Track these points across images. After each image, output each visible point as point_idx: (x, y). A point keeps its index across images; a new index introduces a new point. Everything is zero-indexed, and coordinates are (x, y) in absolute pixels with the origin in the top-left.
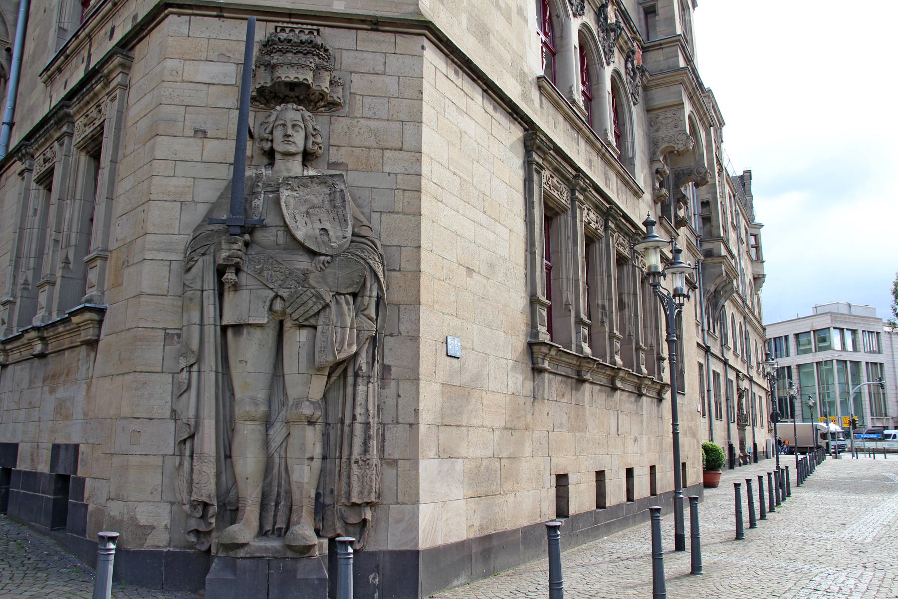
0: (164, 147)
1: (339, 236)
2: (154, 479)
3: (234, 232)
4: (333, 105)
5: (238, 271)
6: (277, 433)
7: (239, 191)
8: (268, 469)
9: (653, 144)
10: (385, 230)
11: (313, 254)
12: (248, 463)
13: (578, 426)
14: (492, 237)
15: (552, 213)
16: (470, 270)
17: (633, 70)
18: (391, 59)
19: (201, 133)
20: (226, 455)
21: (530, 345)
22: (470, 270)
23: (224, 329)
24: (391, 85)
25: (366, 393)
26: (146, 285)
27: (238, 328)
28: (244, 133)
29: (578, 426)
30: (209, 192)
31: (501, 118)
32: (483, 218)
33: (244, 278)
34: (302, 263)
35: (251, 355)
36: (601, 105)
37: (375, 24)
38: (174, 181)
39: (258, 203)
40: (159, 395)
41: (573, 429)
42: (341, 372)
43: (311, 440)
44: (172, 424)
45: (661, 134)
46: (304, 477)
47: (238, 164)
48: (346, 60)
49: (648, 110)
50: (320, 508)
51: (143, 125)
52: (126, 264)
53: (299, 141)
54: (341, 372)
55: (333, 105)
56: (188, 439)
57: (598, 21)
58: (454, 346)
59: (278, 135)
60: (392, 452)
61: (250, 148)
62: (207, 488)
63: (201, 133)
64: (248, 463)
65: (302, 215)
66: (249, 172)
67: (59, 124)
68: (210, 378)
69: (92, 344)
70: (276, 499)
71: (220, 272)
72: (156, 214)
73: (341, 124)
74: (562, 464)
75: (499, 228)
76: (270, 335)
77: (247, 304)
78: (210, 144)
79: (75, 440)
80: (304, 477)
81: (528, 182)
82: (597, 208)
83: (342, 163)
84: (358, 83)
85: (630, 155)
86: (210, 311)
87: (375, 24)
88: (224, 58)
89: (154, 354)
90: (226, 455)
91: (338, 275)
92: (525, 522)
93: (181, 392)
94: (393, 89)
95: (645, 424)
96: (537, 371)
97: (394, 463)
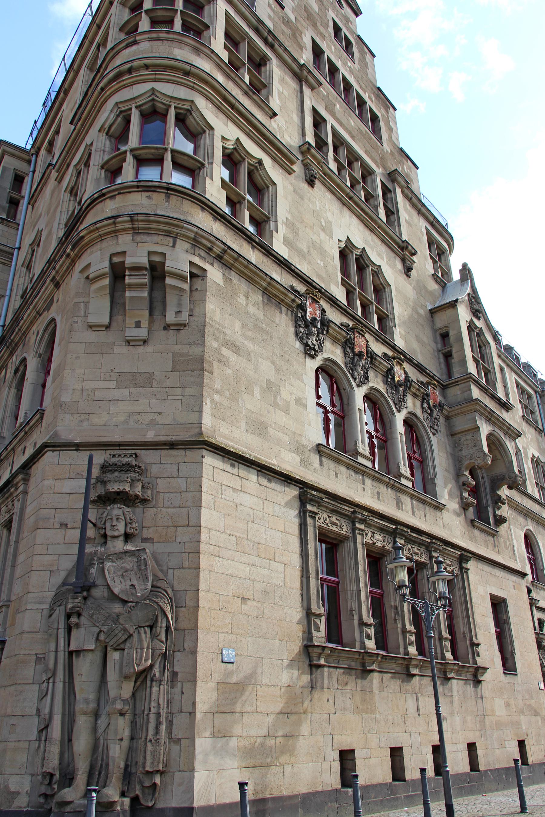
0: (42, 536)
1: (142, 588)
2: (22, 758)
4: (144, 501)
5: (79, 615)
6: (102, 722)
7: (82, 564)
8: (95, 748)
9: (457, 463)
10: (177, 579)
11: (124, 602)
12: (82, 744)
13: (366, 707)
14: (266, 572)
15: (332, 544)
16: (244, 600)
17: (429, 408)
18: (183, 467)
19: (64, 526)
20: (68, 738)
21: (306, 647)
22: (244, 600)
23: (71, 653)
24: (181, 483)
25: (159, 693)
26: (26, 628)
27: (78, 652)
29: (366, 707)
30: (68, 563)
31: (276, 486)
32: (256, 560)
33: (84, 620)
34: (118, 608)
35: (86, 669)
36: (394, 445)
37: (172, 445)
38: (47, 558)
39: (93, 571)
41: (358, 711)
42: (143, 677)
43: (122, 726)
44: (36, 720)
45: (464, 453)
46: (117, 753)
48: (154, 470)
49: (452, 434)
50: (127, 775)
51: (32, 519)
52: (18, 611)
53: (121, 528)
54: (143, 677)
55: (144, 501)
57: (386, 382)
58: (229, 654)
59: (108, 525)
60: (177, 733)
61: (91, 533)
62: (53, 763)
63: (64, 526)
64: (82, 744)
65: (117, 578)
66: (89, 549)
68: (60, 686)
71: (68, 616)
72: (35, 579)
73: (150, 512)
75: (273, 565)
76: (97, 657)
78: (70, 532)
80: (117, 753)
82: (382, 530)
83: (150, 538)
84: (161, 485)
85: (432, 475)
86: (62, 642)
87: (172, 445)
88: (79, 476)
89: (29, 672)
91: (139, 615)
92: (304, 789)
93: (42, 697)
94: (183, 487)
95: (456, 704)
96: (314, 667)
97: (178, 741)
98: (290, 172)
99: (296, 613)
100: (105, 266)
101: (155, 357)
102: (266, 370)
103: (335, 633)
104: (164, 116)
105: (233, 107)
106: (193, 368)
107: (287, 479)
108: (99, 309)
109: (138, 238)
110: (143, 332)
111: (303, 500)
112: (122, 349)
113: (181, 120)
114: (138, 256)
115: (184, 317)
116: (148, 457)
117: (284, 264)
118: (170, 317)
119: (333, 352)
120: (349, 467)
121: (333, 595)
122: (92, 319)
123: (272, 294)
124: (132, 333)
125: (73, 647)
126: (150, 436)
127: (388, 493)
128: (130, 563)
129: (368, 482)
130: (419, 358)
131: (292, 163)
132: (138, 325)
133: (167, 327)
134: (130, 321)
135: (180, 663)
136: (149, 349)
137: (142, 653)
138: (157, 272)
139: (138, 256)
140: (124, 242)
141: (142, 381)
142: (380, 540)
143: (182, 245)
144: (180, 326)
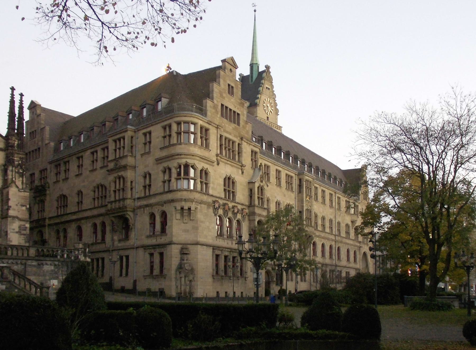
1: (190, 268)
3: (180, 268)
20: (181, 288)
25: (193, 283)
28: (181, 258)
31: (209, 248)
35: (183, 279)
40: (173, 283)
42: (190, 281)
43: (188, 287)
47: (181, 260)
50: (189, 293)
56: (177, 287)
57: (232, 214)
63: (176, 258)
64: (183, 289)
65: (187, 266)
67: (154, 248)
69: (165, 278)
70: (185, 293)
74: (218, 290)
77: (183, 275)
82: (228, 251)
84: (191, 251)
87: (193, 244)
89: (173, 279)
90: (181, 288)
93: (176, 283)
96: (214, 278)
98: (213, 166)
100: (180, 208)
101: (189, 226)
102: (207, 224)
103: (217, 273)
106: (196, 229)
108: (178, 216)
111: (213, 249)
112: (183, 224)
113: (192, 167)
114: (186, 208)
115: (194, 218)
116: (189, 246)
117: (212, 196)
118: (191, 218)
119: (221, 212)
121: (217, 265)
122: (177, 218)
123: (208, 205)
124: (185, 221)
126: (189, 242)
127: (230, 242)
128: (188, 264)
129: (226, 240)
130: (243, 202)
133: (191, 220)
134: (184, 219)
135: (195, 278)
136: (187, 225)
137: (191, 277)
138: (189, 209)
139: (186, 208)
140: (183, 204)
141: (186, 231)
142: (227, 254)
143: (194, 203)
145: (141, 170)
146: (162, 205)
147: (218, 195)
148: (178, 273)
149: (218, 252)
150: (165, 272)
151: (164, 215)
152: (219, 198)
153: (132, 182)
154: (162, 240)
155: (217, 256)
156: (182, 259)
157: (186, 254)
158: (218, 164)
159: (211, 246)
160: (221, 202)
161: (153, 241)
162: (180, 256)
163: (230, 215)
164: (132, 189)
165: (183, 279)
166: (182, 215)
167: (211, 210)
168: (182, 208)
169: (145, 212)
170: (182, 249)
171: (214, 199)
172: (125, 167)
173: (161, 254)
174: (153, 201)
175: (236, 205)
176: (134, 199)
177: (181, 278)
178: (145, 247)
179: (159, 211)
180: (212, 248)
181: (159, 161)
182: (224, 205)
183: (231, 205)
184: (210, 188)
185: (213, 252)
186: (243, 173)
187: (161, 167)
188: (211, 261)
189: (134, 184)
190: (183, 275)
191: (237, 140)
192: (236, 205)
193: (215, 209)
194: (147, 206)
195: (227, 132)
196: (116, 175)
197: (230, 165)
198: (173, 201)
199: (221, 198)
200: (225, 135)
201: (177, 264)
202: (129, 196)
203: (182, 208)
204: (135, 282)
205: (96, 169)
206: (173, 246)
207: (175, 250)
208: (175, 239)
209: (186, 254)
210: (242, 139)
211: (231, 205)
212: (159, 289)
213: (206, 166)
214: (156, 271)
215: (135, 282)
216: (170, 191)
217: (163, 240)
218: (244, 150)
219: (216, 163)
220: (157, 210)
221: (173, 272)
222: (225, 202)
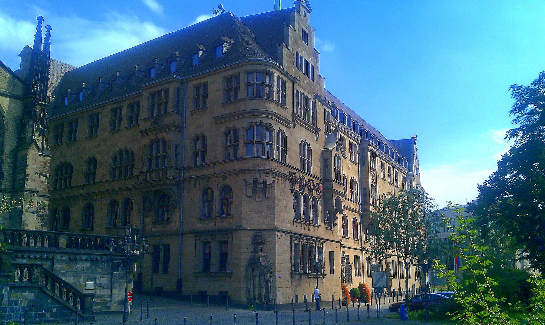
3: (253, 263)
4: (264, 243)
31: (287, 235)
34: (263, 268)
35: (257, 279)
37: (269, 230)
40: (244, 285)
56: (249, 290)
64: (257, 293)
69: (230, 277)
70: (260, 297)
72: (242, 260)
77: (257, 273)
79: (226, 290)
81: (291, 243)
93: (247, 284)
96: (292, 277)
99: (290, 266)
104: (263, 126)
105: (280, 119)
106: (272, 209)
107: (288, 233)
108: (250, 192)
109: (261, 175)
110: (260, 199)
111: (291, 237)
112: (255, 203)
115: (270, 195)
116: (264, 232)
117: (289, 166)
118: (267, 195)
119: (297, 187)
120: (299, 223)
122: (248, 194)
124: (258, 199)
125: (254, 275)
131: (289, 124)
132: (259, 197)
133: (266, 197)
134: (257, 196)
135: (273, 278)
138: (265, 182)
140: (257, 175)
144: (269, 197)
145: (191, 131)
146: (226, 178)
147: (294, 166)
148: (250, 269)
149: (296, 241)
150: (229, 268)
151: (226, 190)
152: (295, 169)
153: (176, 147)
154: (225, 223)
155: (295, 245)
156: (256, 251)
157: (261, 243)
158: (294, 127)
159: (288, 233)
160: (298, 174)
161: (211, 226)
162: (252, 246)
163: (306, 191)
164: (176, 155)
165: (257, 279)
166: (255, 191)
167: (288, 185)
168: (255, 182)
169: (197, 186)
170: (255, 236)
171: (291, 171)
172: (168, 128)
173: (223, 243)
174: (209, 171)
175: (312, 178)
176: (180, 170)
177: (254, 277)
178: (197, 234)
179: (219, 186)
180: (290, 235)
181: (219, 120)
182: (302, 178)
183: (307, 178)
184: (287, 156)
185: (291, 240)
186: (317, 138)
187: (223, 129)
188: (290, 253)
189: (179, 150)
190: (257, 273)
191: (311, 97)
192: (312, 178)
193: (292, 184)
194: (200, 178)
195: (302, 87)
196: (153, 138)
197: (305, 128)
198: (243, 171)
199: (298, 170)
200: (300, 90)
201: (248, 257)
202: (173, 165)
203: (255, 182)
204: (180, 281)
205: (120, 129)
206: (243, 232)
207: (245, 240)
208: (245, 225)
209: (261, 243)
210: (316, 97)
211: (307, 178)
212: (221, 292)
213: (283, 128)
214: (214, 267)
215: (180, 281)
216: (237, 159)
217: (225, 224)
218: (318, 111)
219: (291, 125)
220: (216, 183)
221: (243, 268)
222: (301, 174)
